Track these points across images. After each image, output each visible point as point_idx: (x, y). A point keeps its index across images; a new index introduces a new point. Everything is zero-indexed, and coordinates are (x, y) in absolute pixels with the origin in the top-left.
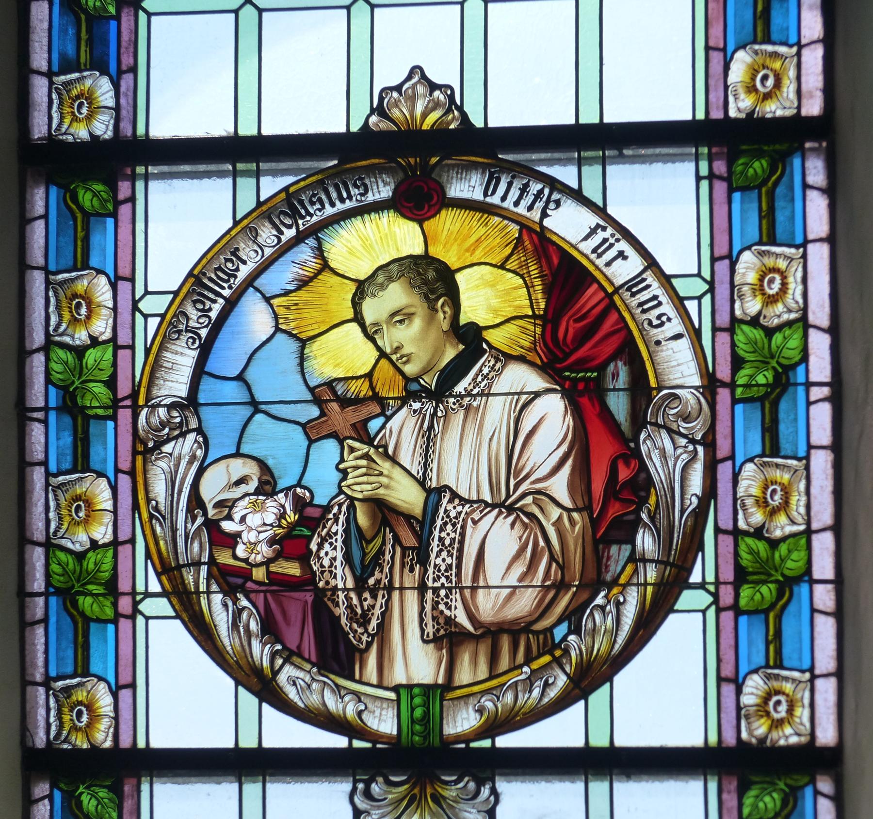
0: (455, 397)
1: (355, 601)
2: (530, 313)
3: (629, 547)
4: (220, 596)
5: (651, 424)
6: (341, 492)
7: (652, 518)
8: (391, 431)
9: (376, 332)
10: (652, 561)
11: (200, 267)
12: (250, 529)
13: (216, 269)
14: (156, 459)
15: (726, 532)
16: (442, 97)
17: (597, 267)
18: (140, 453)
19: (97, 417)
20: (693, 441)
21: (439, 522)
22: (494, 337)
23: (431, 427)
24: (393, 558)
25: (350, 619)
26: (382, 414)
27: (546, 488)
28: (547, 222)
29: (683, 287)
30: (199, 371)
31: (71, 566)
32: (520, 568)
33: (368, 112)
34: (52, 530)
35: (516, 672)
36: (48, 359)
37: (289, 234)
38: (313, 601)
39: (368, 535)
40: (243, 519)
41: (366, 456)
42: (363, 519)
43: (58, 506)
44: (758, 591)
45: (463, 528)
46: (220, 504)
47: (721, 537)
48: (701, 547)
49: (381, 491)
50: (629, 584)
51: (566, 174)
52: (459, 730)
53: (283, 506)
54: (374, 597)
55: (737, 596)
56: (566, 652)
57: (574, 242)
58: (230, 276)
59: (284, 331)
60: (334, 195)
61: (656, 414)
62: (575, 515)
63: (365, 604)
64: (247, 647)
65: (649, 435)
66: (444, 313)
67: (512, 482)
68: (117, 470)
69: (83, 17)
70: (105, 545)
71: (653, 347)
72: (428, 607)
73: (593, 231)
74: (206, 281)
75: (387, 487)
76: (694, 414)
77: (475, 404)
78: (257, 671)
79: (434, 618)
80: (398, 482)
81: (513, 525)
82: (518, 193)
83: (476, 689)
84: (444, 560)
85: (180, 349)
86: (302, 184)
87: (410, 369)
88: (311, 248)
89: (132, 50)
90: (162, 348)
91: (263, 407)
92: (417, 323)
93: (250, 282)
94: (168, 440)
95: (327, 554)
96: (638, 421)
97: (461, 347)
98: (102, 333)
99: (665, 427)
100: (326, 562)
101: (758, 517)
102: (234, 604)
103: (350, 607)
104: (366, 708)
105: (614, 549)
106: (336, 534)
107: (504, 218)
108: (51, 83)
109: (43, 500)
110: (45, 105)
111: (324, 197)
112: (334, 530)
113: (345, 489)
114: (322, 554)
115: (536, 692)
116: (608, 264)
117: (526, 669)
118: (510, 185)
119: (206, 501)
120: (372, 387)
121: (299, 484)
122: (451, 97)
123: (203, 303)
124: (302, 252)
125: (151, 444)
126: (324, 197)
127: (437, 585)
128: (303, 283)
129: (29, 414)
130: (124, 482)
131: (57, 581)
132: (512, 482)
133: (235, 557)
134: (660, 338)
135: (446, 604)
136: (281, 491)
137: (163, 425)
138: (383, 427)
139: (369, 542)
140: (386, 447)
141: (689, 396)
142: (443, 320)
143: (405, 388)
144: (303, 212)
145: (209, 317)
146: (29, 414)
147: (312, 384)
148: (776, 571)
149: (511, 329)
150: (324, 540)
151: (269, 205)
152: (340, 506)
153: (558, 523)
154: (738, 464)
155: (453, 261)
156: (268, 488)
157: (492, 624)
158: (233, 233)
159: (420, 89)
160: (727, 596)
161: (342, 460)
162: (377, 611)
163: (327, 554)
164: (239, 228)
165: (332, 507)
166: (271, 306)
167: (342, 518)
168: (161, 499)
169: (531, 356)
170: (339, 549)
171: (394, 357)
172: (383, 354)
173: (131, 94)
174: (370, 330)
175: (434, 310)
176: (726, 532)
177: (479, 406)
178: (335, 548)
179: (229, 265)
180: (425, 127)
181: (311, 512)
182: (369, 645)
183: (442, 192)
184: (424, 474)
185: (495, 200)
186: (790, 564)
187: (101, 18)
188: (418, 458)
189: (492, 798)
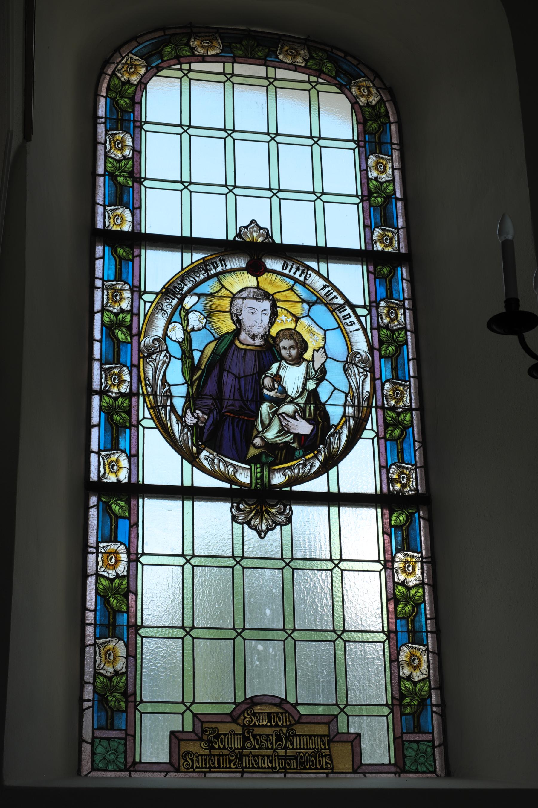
7: (352, 400)
18: (141, 358)
48: (371, 413)
51: (313, 265)
65: (349, 367)
71: (350, 334)
73: (325, 287)
99: (355, 364)
118: (292, 267)
130: (135, 370)
145: (172, 306)
168: (151, 378)
185: (287, 272)
187: (126, 186)
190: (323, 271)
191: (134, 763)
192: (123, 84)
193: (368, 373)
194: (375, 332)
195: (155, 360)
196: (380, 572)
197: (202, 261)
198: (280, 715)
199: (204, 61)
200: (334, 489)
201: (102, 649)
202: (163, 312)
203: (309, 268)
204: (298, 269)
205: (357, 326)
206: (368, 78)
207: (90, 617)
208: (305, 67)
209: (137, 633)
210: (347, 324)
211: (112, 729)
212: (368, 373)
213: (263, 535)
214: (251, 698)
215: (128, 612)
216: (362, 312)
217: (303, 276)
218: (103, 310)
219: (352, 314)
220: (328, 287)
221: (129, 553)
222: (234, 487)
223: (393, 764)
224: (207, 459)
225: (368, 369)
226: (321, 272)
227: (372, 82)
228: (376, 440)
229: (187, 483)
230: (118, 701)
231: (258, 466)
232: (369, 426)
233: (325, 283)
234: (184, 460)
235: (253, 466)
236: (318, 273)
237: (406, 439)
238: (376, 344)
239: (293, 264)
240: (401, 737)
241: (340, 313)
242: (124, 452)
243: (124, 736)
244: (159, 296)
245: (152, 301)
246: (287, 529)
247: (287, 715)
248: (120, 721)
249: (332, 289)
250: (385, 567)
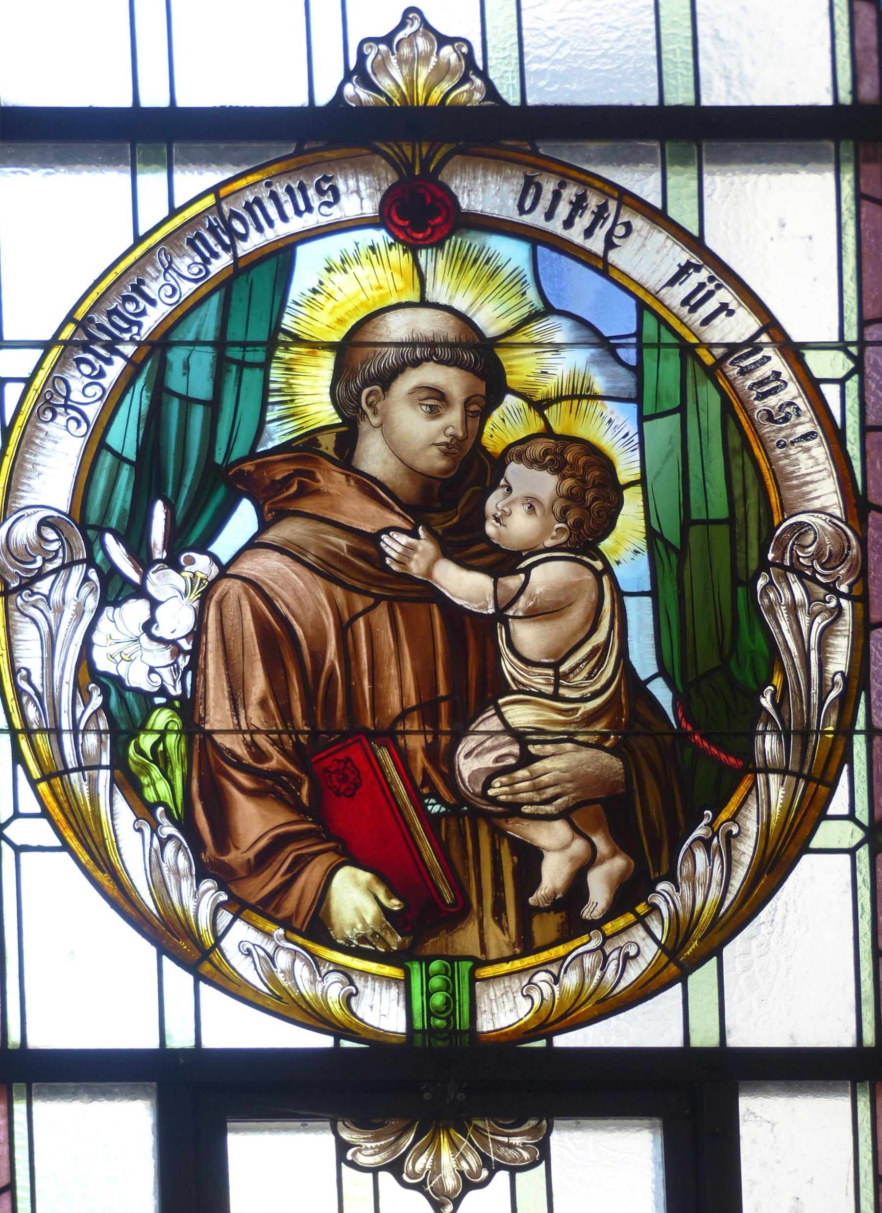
33: (341, 77)
48: (848, 758)
73: (684, 271)
94: (40, 575)
116: (706, 321)
118: (557, 196)
122: (469, 58)
179: (131, 307)
185: (536, 219)
193: (845, 604)
195: (48, 598)
197: (210, 200)
202: (73, 413)
204: (578, 205)
205: (806, 424)
217: (600, 233)
220: (698, 268)
222: (345, 1044)
224: (249, 953)
225: (844, 588)
226: (672, 213)
231: (435, 966)
232: (839, 804)
233: (682, 255)
235: (415, 967)
239: (562, 185)
244: (55, 352)
245: (26, 374)
249: (711, 279)
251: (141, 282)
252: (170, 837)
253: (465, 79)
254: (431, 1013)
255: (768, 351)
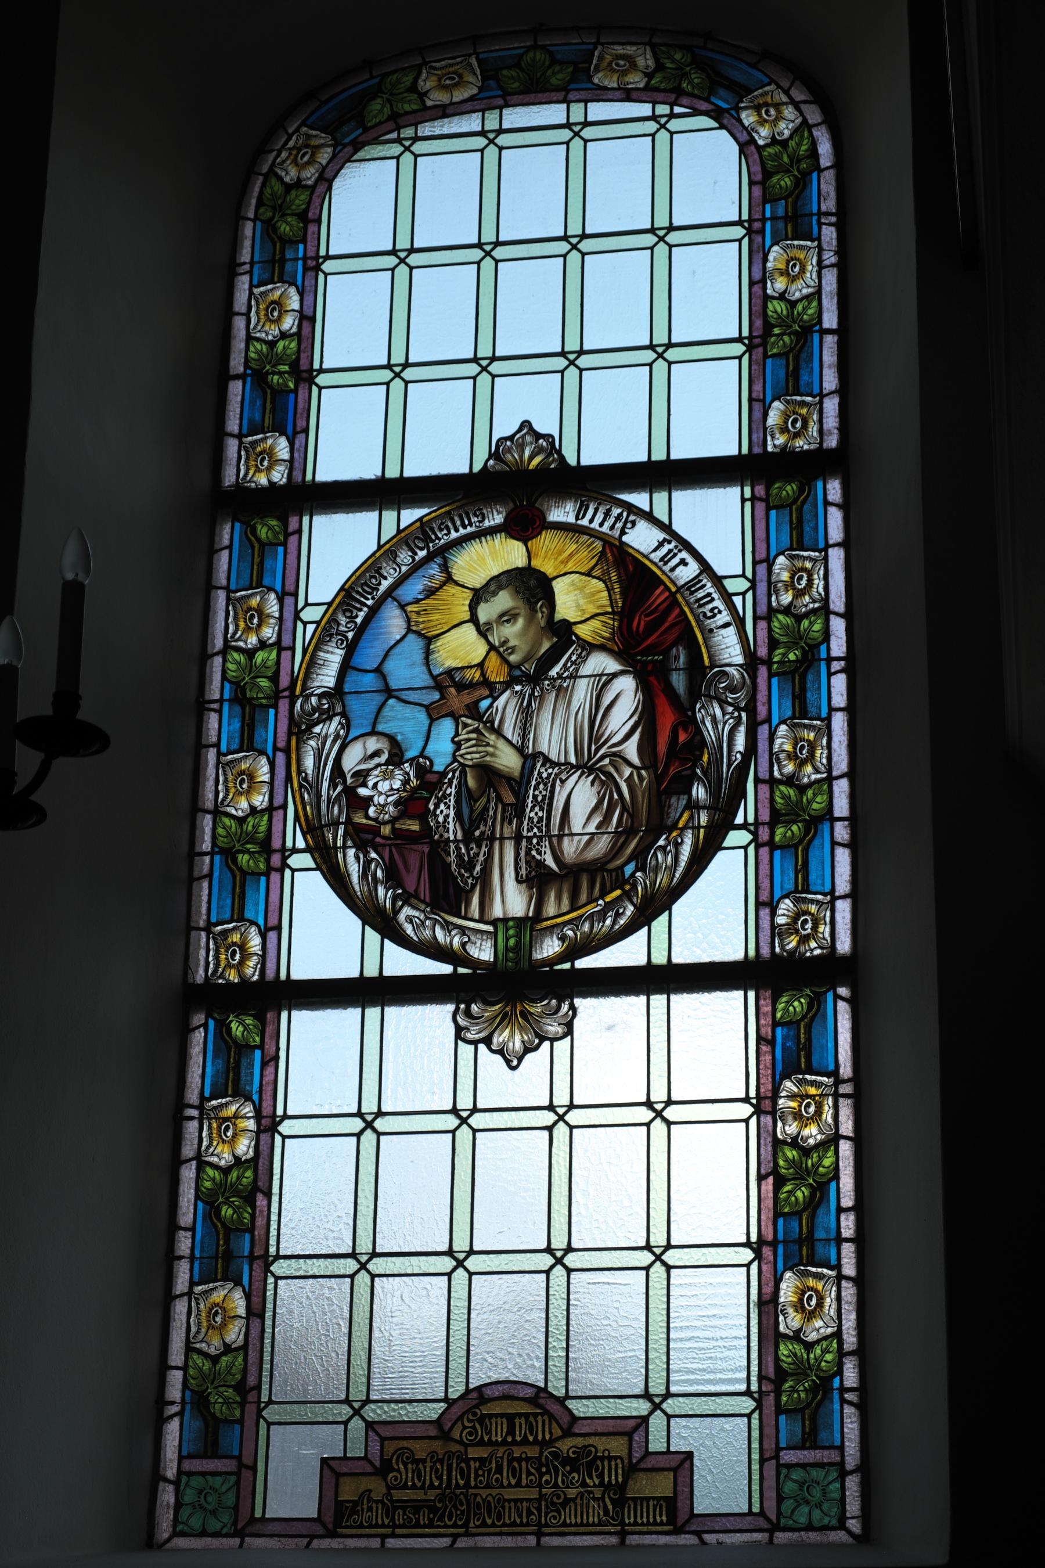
0: (549, 679)
1: (463, 851)
2: (610, 610)
3: (686, 797)
4: (354, 850)
5: (705, 696)
6: (455, 760)
7: (704, 772)
8: (497, 709)
9: (488, 630)
10: (704, 808)
11: (350, 583)
12: (380, 794)
13: (363, 584)
14: (308, 739)
15: (764, 781)
16: (544, 444)
17: (664, 573)
18: (294, 734)
19: (262, 706)
20: (738, 709)
21: (533, 783)
22: (584, 631)
23: (529, 704)
24: (495, 813)
25: (459, 866)
26: (490, 696)
27: (620, 751)
28: (625, 538)
29: (731, 586)
30: (346, 667)
31: (233, 829)
32: (597, 819)
33: (487, 456)
34: (220, 800)
35: (593, 905)
36: (225, 661)
37: (422, 554)
38: (429, 852)
39: (476, 795)
40: (375, 786)
41: (476, 731)
42: (471, 782)
43: (226, 780)
44: (790, 829)
45: (553, 786)
46: (357, 774)
47: (760, 786)
48: (744, 796)
49: (488, 759)
50: (685, 827)
52: (545, 955)
53: (408, 774)
54: (479, 847)
55: (772, 834)
56: (634, 886)
57: (645, 552)
58: (373, 589)
59: (415, 632)
60: (458, 523)
61: (708, 688)
62: (643, 772)
63: (472, 852)
64: (372, 889)
66: (542, 612)
67: (593, 748)
68: (275, 749)
69: (269, 391)
70: (262, 811)
72: (522, 853)
73: (661, 544)
74: (354, 594)
75: (493, 755)
76: (739, 686)
77: (565, 685)
78: (381, 910)
79: (527, 862)
80: (501, 751)
81: (592, 783)
82: (602, 516)
83: (559, 920)
84: (536, 814)
85: (331, 649)
86: (434, 515)
87: (513, 658)
88: (438, 565)
89: (305, 415)
90: (317, 648)
91: (396, 693)
92: (520, 622)
93: (390, 592)
94: (317, 724)
95: (442, 812)
96: (695, 694)
97: (555, 639)
98: (269, 638)
100: (441, 819)
101: (790, 768)
102: (365, 856)
103: (459, 856)
104: (469, 939)
105: (674, 800)
106: (450, 795)
107: (592, 536)
108: (241, 443)
109: (214, 775)
110: (234, 462)
111: (450, 524)
112: (448, 792)
113: (459, 758)
114: (438, 812)
115: (608, 922)
116: (673, 569)
117: (601, 902)
118: (596, 510)
119: (346, 771)
120: (483, 674)
121: (422, 755)
123: (352, 612)
124: (432, 568)
125: (303, 727)
126: (450, 524)
127: (530, 834)
128: (430, 592)
129: (207, 706)
130: (280, 758)
131: (222, 842)
132: (593, 748)
133: (367, 817)
134: (713, 626)
135: (537, 850)
136: (407, 762)
137: (314, 710)
138: (491, 706)
139: (476, 801)
140: (492, 722)
141: (735, 673)
142: (541, 618)
143: (509, 674)
144: (433, 537)
145: (356, 623)
146: (207, 706)
147: (435, 672)
148: (804, 812)
149: (595, 624)
150: (439, 801)
151: (407, 532)
152: (454, 772)
153: (629, 780)
154: (774, 726)
155: (549, 569)
156: (396, 759)
157: (574, 865)
158: (378, 555)
159: (528, 438)
160: (764, 834)
161: (457, 734)
162: (481, 858)
163: (442, 812)
164: (382, 551)
165: (448, 774)
166: (405, 612)
167: (455, 782)
168: (310, 772)
169: (610, 644)
170: (452, 808)
171: (501, 650)
172: (492, 647)
173: (302, 449)
174: (483, 629)
175: (533, 610)
176: (764, 781)
177: (568, 686)
178: (449, 807)
180: (531, 467)
181: (433, 778)
182: (473, 886)
183: (543, 516)
184: (522, 743)
185: (585, 522)
186: (815, 806)
187: (282, 391)
188: (518, 731)
189: (570, 1013)
190: (661, 514)
191: (253, 1520)
192: (288, 188)
194: (762, 625)
196: (746, 1121)
198: (531, 1419)
199: (445, 115)
200: (659, 958)
201: (201, 1301)
203: (630, 508)
205: (724, 617)
206: (779, 86)
207: (184, 1244)
208: (647, 88)
209: (267, 1270)
210: (705, 614)
211: (215, 1456)
212: (744, 715)
213: (515, 1063)
214: (479, 1388)
215: (251, 1230)
216: (733, 586)
218: (227, 648)
219: (715, 596)
220: (669, 542)
221: (258, 1116)
222: (461, 970)
223: (755, 1514)
224: (411, 922)
227: (786, 92)
228: (751, 850)
229: (371, 971)
230: (226, 1402)
233: (661, 536)
234: (367, 927)
236: (649, 516)
237: (816, 842)
238: (763, 652)
240: (777, 1457)
241: (692, 593)
242: (253, 923)
243: (234, 1469)
245: (318, 618)
246: (562, 1047)
247: (546, 1417)
248: (230, 1438)
249: (676, 547)
250: (758, 1111)
251: (380, 568)
252: (373, 859)
253: (550, 454)
254: (507, 949)
255: (705, 581)
